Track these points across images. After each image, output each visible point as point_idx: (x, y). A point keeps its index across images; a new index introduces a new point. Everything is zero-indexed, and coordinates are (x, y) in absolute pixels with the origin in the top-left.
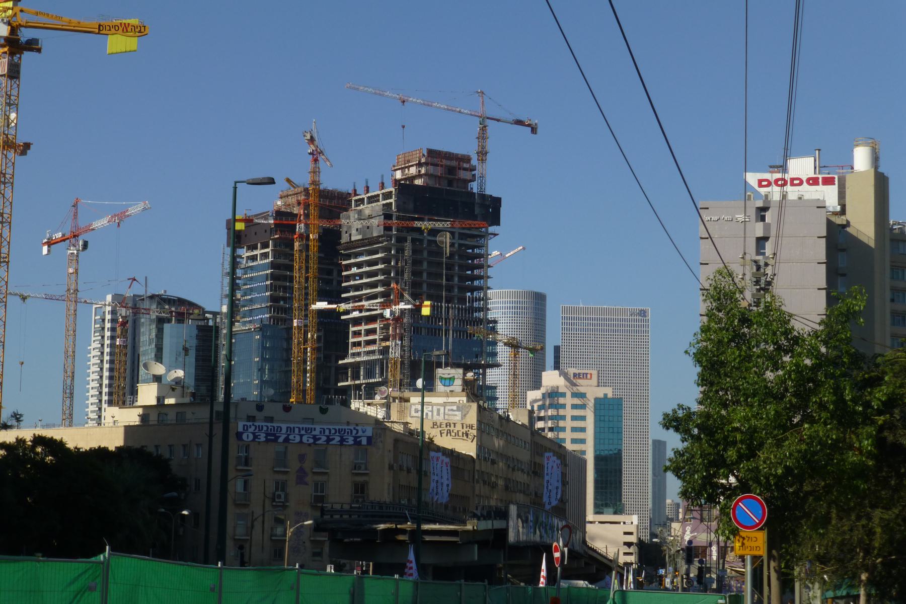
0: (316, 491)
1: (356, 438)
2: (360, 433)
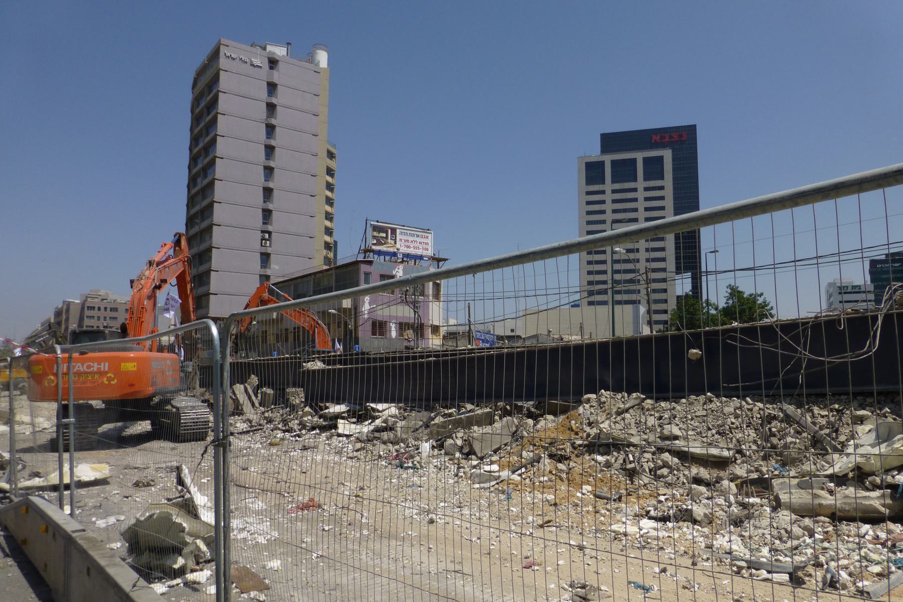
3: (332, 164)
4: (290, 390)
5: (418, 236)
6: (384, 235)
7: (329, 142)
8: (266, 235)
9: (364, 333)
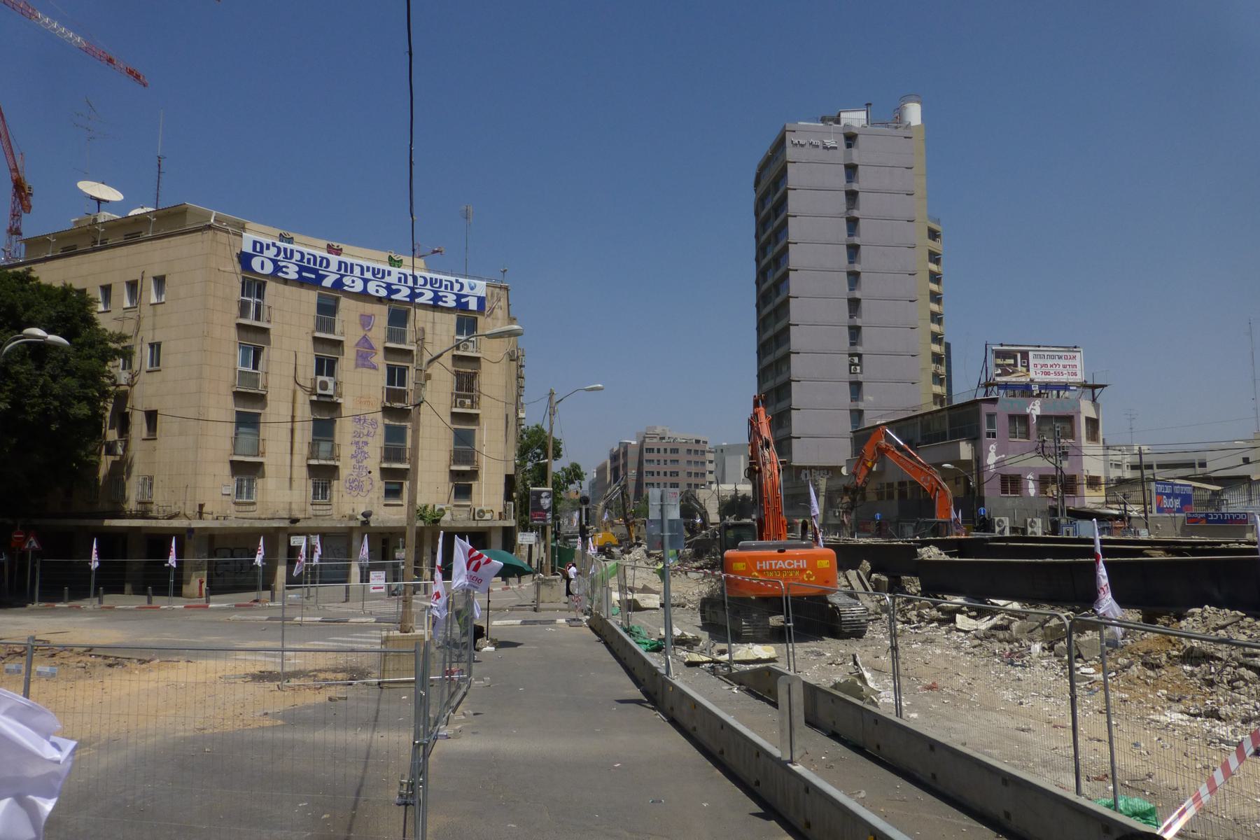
0: (391, 381)
1: (459, 297)
2: (466, 291)
3: (935, 246)
4: (904, 578)
5: (1060, 358)
6: (1012, 361)
7: (930, 218)
8: (856, 359)
9: (991, 492)
